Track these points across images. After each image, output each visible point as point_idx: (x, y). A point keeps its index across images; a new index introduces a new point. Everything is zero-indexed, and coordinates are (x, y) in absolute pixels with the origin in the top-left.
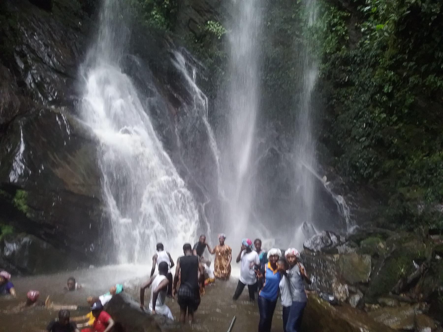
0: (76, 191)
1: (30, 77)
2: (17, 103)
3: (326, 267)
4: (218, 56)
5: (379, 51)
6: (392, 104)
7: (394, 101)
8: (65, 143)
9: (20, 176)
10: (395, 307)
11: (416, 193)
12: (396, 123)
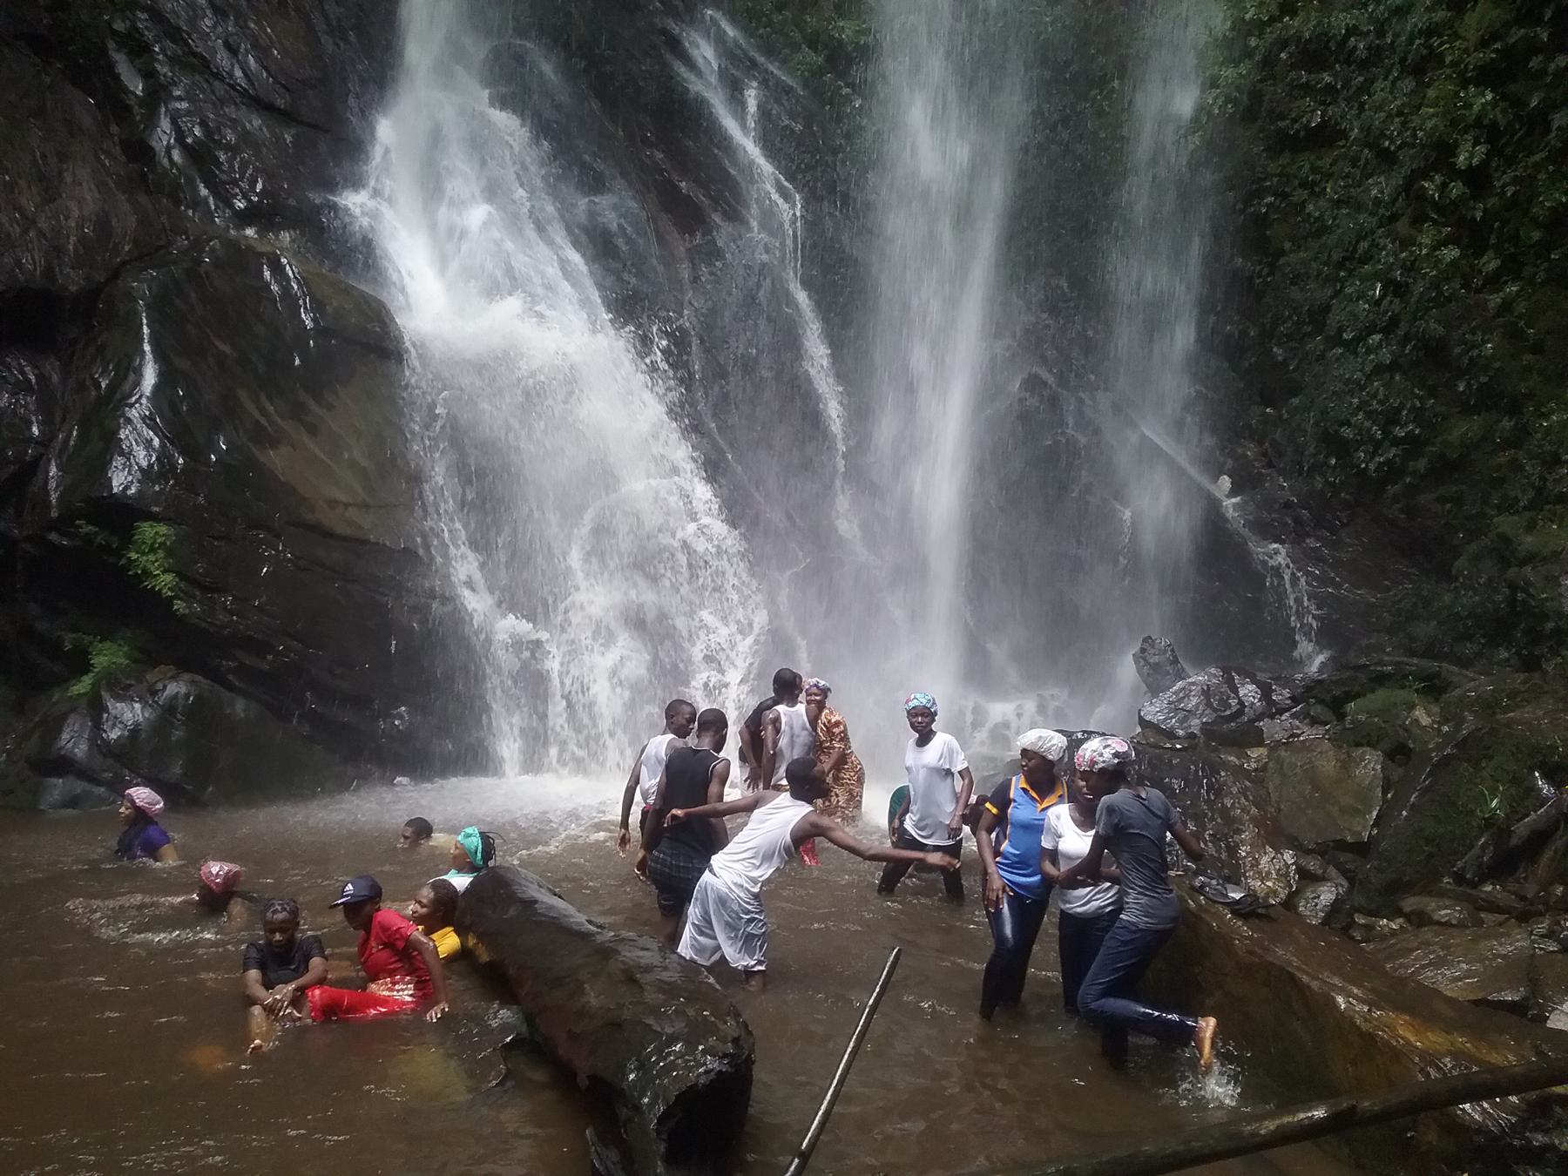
0: (341, 529)
1: (165, 124)
2: (125, 220)
3: (1218, 791)
4: (840, 41)
5: (1441, 15)
6: (1485, 211)
7: (1493, 201)
8: (297, 362)
9: (146, 473)
10: (1461, 925)
11: (1560, 535)
12: (1494, 282)
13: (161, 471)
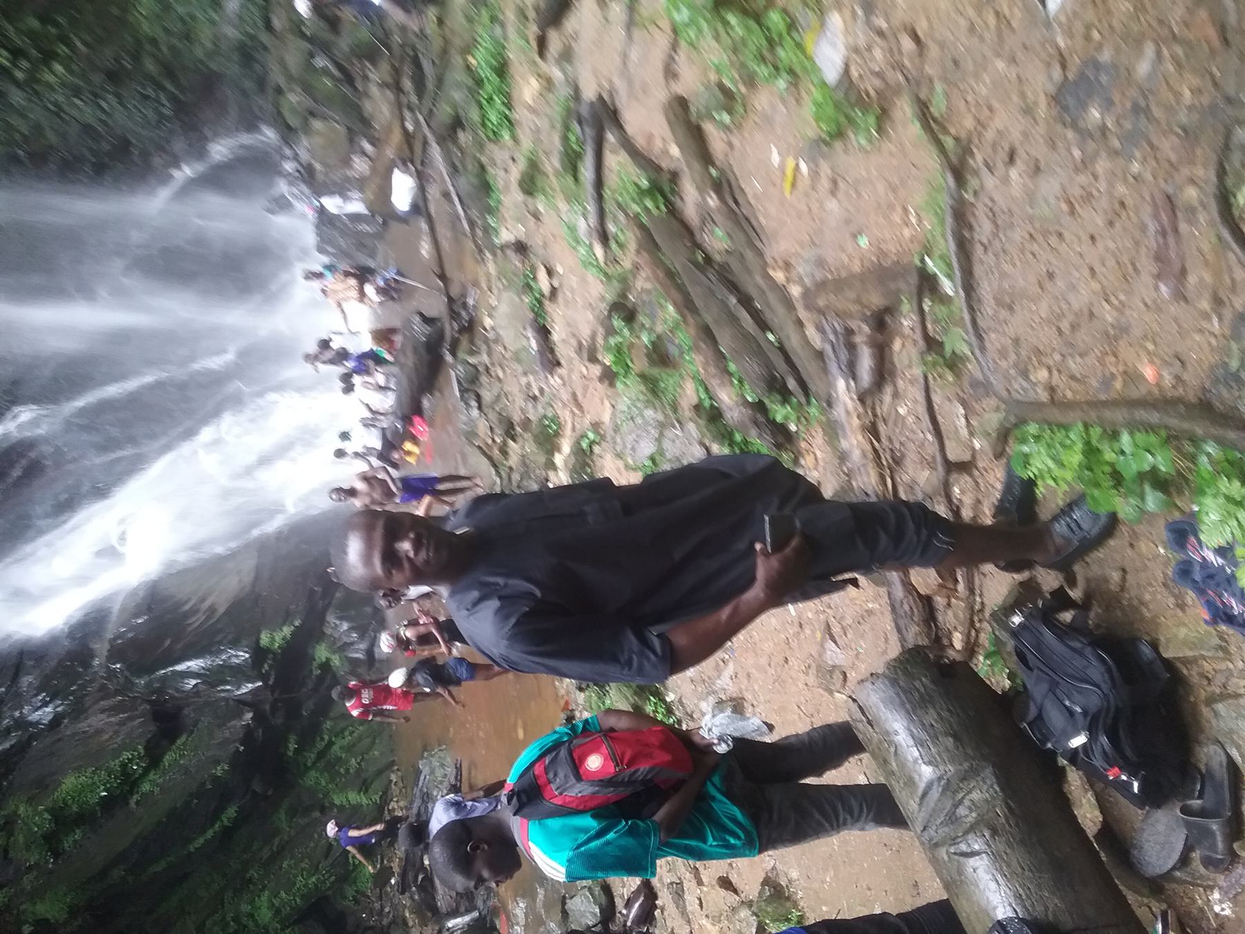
11: (205, 35)
13: (235, 644)
